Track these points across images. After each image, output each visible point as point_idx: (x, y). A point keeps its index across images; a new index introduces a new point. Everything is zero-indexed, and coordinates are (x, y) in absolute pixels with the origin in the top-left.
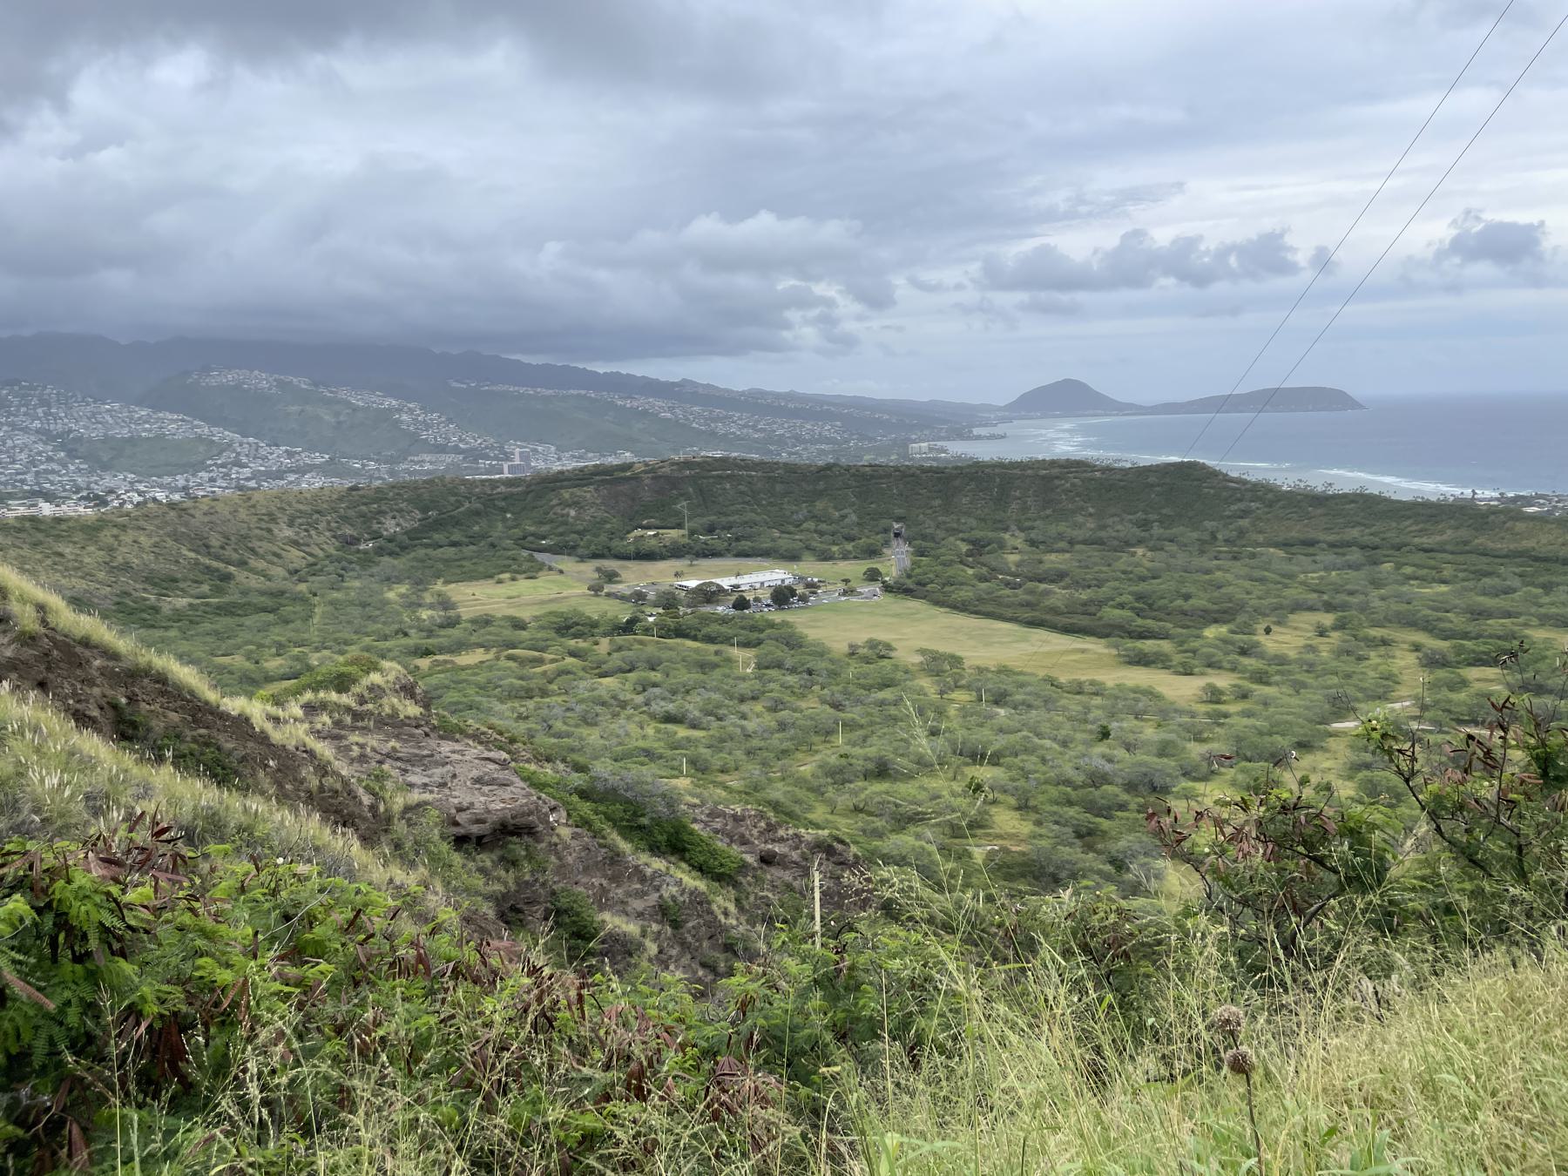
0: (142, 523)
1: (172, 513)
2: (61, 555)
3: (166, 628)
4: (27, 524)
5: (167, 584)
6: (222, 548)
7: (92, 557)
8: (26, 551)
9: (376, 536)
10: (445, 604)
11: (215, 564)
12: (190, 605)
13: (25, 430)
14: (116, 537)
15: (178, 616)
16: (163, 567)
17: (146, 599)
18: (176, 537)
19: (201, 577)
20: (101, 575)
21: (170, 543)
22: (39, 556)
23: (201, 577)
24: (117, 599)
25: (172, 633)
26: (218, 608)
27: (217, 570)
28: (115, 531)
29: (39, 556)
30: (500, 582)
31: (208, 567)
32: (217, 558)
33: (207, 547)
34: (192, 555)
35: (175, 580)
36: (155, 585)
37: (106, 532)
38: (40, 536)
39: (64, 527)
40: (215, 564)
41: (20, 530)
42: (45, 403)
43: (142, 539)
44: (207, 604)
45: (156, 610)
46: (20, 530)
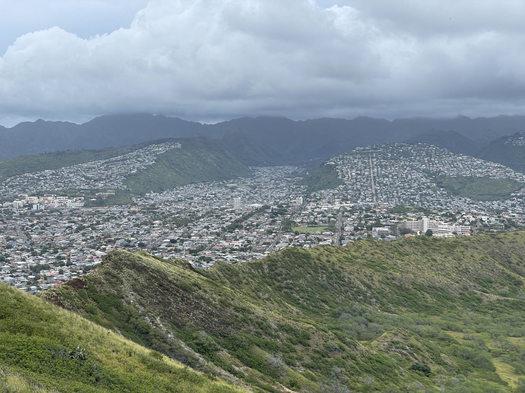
0: (476, 245)
1: (493, 240)
2: (435, 260)
3: (485, 313)
4: (421, 241)
5: (486, 284)
6: (518, 264)
7: (450, 263)
8: (419, 257)
11: (513, 274)
12: (498, 300)
13: (418, 170)
14: (462, 252)
15: (491, 306)
16: (485, 273)
17: (476, 293)
18: (493, 255)
19: (505, 282)
20: (454, 275)
21: (490, 259)
22: (425, 260)
23: (505, 282)
24: (461, 291)
25: (488, 318)
26: (513, 304)
27: (514, 278)
28: (462, 249)
29: (425, 260)
31: (509, 276)
32: (515, 270)
33: (510, 263)
34: (501, 267)
35: (491, 282)
36: (480, 284)
37: (458, 249)
38: (426, 248)
39: (437, 244)
40: (513, 274)
41: (417, 244)
42: (429, 155)
43: (476, 255)
44: (507, 301)
45: (480, 300)
46: (417, 244)
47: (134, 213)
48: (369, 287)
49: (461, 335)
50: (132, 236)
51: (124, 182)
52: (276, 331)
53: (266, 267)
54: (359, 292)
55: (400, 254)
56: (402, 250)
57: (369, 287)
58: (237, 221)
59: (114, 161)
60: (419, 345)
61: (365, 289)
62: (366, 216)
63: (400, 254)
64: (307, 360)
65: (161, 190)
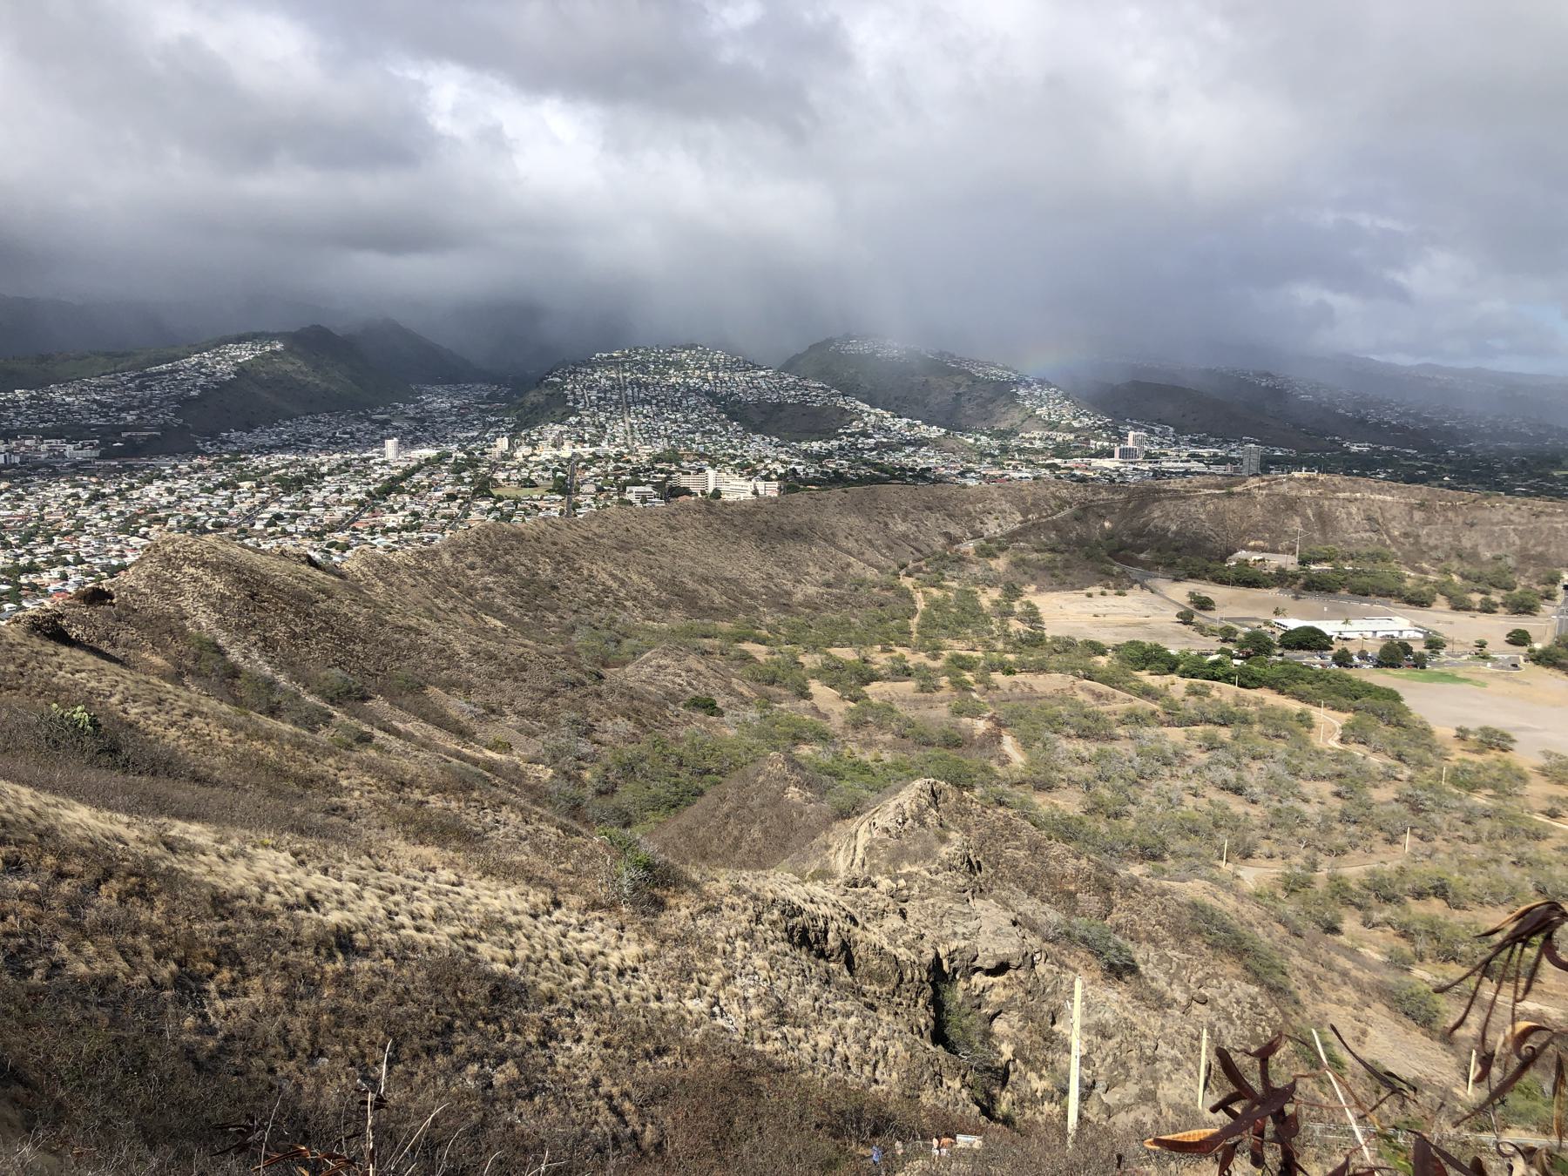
9: (977, 535)
10: (1032, 616)
30: (1090, 595)
47: (201, 468)
48: (623, 584)
49: (763, 648)
50: (199, 509)
51: (177, 412)
52: (468, 660)
53: (446, 556)
54: (607, 590)
55: (673, 528)
56: (673, 522)
57: (623, 584)
58: (393, 479)
59: (153, 374)
60: (701, 668)
61: (615, 586)
62: (617, 468)
63: (673, 528)
64: (521, 704)
65: (249, 427)
